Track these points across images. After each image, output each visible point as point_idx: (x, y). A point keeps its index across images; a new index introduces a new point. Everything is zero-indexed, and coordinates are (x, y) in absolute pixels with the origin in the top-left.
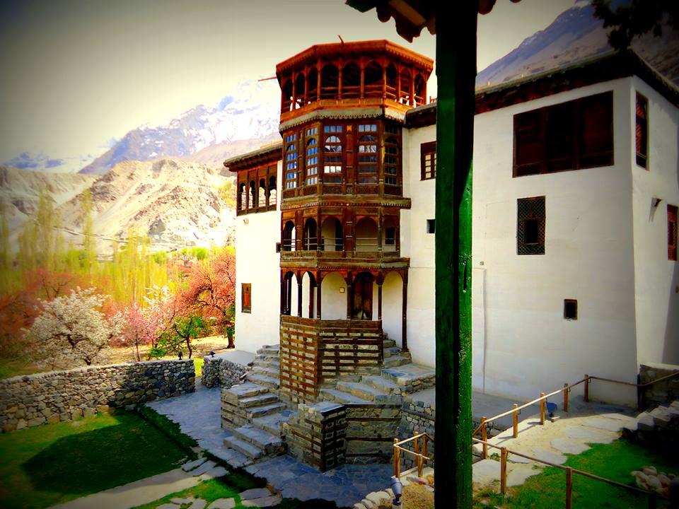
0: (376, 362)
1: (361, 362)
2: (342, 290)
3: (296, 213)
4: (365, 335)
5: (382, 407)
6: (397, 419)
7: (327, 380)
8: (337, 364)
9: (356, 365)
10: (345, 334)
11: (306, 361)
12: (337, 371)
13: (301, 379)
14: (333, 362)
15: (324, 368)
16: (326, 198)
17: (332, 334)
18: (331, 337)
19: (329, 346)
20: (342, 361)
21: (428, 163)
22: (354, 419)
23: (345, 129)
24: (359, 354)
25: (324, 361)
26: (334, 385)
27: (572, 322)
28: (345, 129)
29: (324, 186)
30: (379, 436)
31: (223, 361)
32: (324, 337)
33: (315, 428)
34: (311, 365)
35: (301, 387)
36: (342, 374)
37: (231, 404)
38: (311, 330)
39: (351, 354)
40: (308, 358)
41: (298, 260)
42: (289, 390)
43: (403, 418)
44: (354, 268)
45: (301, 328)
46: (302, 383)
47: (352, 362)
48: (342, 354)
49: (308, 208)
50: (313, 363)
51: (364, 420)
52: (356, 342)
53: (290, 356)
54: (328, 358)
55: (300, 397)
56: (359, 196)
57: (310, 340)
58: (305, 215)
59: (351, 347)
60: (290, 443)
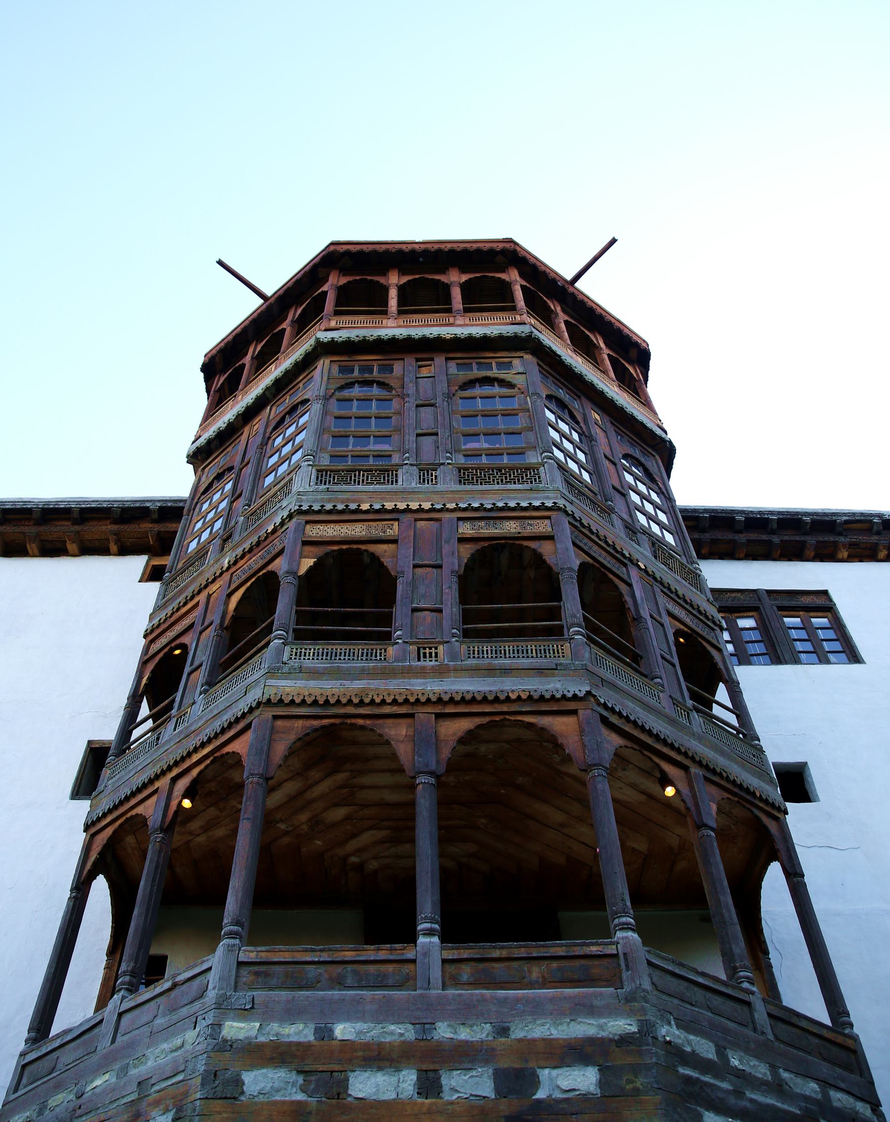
17: (706, 1049)
45: (466, 1013)
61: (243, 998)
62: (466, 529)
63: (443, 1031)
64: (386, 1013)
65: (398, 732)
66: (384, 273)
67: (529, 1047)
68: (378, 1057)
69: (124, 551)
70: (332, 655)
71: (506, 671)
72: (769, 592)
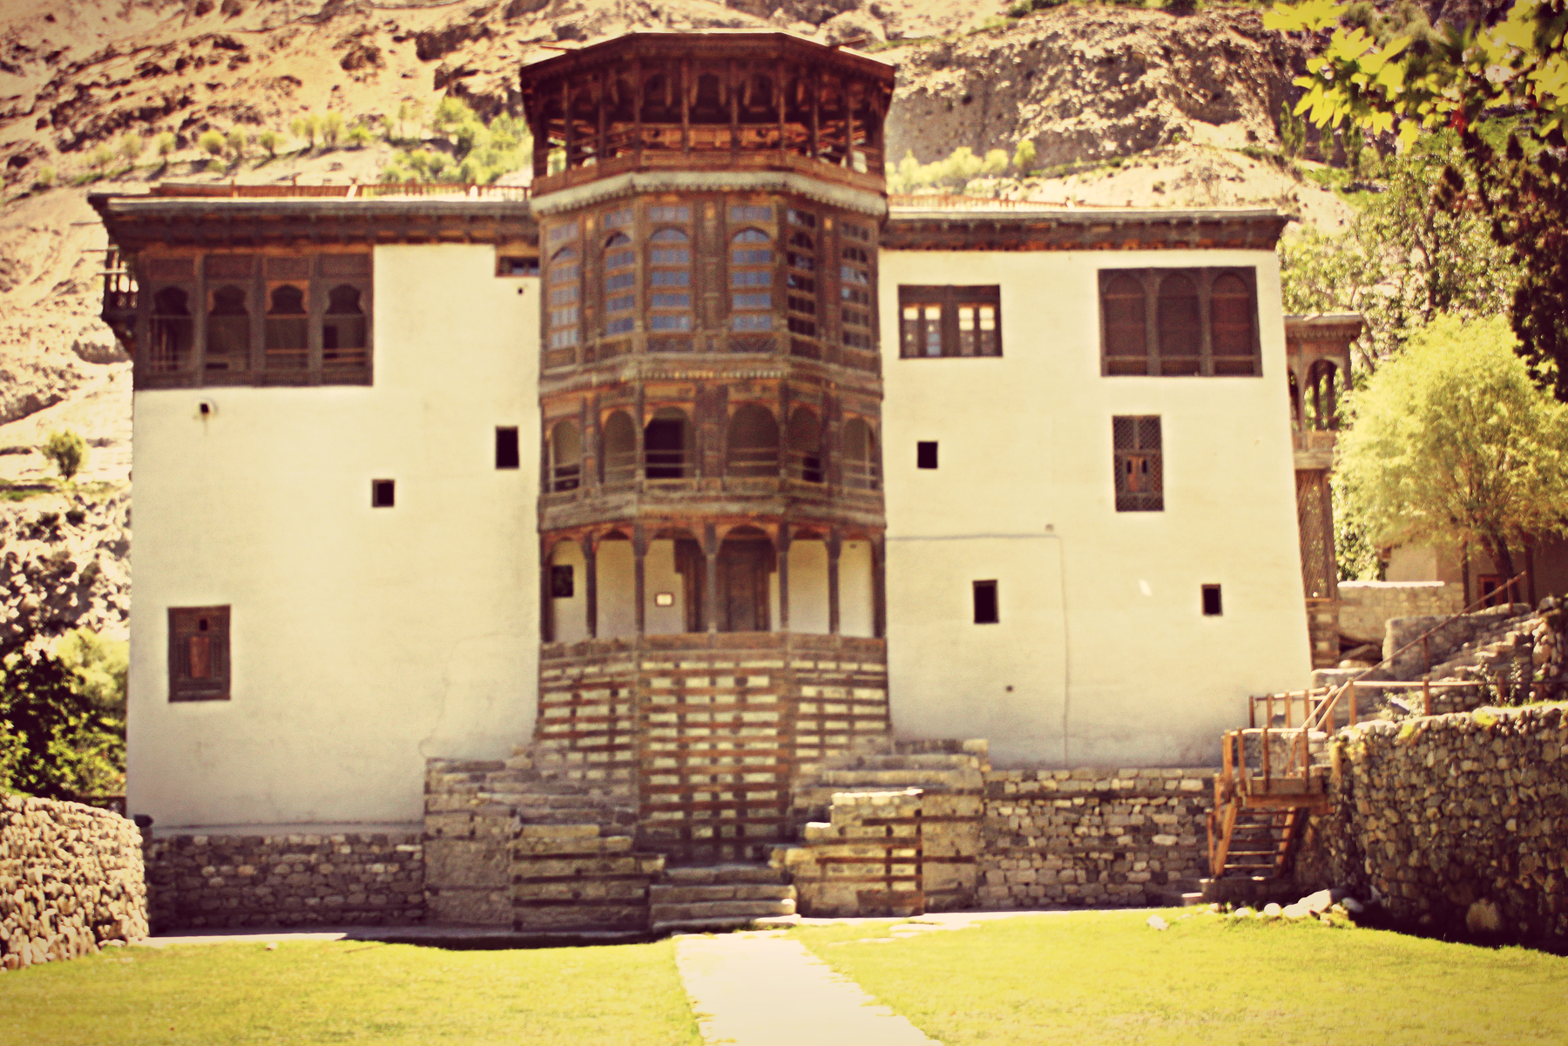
0: (880, 725)
1: (860, 725)
2: (664, 600)
3: (700, 390)
4: (867, 667)
5: (960, 792)
7: (807, 768)
8: (821, 732)
10: (832, 665)
11: (744, 732)
14: (812, 725)
15: (801, 740)
16: (800, 366)
17: (809, 665)
19: (809, 691)
20: (830, 725)
24: (857, 710)
25: (801, 725)
27: (1214, 619)
29: (794, 343)
30: (958, 852)
32: (799, 670)
34: (766, 739)
35: (727, 796)
38: (764, 657)
39: (842, 709)
40: (751, 725)
41: (717, 499)
42: (679, 815)
43: (992, 814)
45: (725, 658)
46: (728, 788)
47: (843, 725)
48: (830, 709)
50: (772, 732)
51: (935, 819)
52: (851, 682)
53: (680, 731)
54: (806, 717)
55: (727, 821)
57: (763, 681)
58: (734, 395)
59: (840, 693)
63: (719, 665)
64: (699, 659)
65: (699, 532)
68: (695, 673)
69: (474, 241)
70: (667, 488)
71: (748, 499)
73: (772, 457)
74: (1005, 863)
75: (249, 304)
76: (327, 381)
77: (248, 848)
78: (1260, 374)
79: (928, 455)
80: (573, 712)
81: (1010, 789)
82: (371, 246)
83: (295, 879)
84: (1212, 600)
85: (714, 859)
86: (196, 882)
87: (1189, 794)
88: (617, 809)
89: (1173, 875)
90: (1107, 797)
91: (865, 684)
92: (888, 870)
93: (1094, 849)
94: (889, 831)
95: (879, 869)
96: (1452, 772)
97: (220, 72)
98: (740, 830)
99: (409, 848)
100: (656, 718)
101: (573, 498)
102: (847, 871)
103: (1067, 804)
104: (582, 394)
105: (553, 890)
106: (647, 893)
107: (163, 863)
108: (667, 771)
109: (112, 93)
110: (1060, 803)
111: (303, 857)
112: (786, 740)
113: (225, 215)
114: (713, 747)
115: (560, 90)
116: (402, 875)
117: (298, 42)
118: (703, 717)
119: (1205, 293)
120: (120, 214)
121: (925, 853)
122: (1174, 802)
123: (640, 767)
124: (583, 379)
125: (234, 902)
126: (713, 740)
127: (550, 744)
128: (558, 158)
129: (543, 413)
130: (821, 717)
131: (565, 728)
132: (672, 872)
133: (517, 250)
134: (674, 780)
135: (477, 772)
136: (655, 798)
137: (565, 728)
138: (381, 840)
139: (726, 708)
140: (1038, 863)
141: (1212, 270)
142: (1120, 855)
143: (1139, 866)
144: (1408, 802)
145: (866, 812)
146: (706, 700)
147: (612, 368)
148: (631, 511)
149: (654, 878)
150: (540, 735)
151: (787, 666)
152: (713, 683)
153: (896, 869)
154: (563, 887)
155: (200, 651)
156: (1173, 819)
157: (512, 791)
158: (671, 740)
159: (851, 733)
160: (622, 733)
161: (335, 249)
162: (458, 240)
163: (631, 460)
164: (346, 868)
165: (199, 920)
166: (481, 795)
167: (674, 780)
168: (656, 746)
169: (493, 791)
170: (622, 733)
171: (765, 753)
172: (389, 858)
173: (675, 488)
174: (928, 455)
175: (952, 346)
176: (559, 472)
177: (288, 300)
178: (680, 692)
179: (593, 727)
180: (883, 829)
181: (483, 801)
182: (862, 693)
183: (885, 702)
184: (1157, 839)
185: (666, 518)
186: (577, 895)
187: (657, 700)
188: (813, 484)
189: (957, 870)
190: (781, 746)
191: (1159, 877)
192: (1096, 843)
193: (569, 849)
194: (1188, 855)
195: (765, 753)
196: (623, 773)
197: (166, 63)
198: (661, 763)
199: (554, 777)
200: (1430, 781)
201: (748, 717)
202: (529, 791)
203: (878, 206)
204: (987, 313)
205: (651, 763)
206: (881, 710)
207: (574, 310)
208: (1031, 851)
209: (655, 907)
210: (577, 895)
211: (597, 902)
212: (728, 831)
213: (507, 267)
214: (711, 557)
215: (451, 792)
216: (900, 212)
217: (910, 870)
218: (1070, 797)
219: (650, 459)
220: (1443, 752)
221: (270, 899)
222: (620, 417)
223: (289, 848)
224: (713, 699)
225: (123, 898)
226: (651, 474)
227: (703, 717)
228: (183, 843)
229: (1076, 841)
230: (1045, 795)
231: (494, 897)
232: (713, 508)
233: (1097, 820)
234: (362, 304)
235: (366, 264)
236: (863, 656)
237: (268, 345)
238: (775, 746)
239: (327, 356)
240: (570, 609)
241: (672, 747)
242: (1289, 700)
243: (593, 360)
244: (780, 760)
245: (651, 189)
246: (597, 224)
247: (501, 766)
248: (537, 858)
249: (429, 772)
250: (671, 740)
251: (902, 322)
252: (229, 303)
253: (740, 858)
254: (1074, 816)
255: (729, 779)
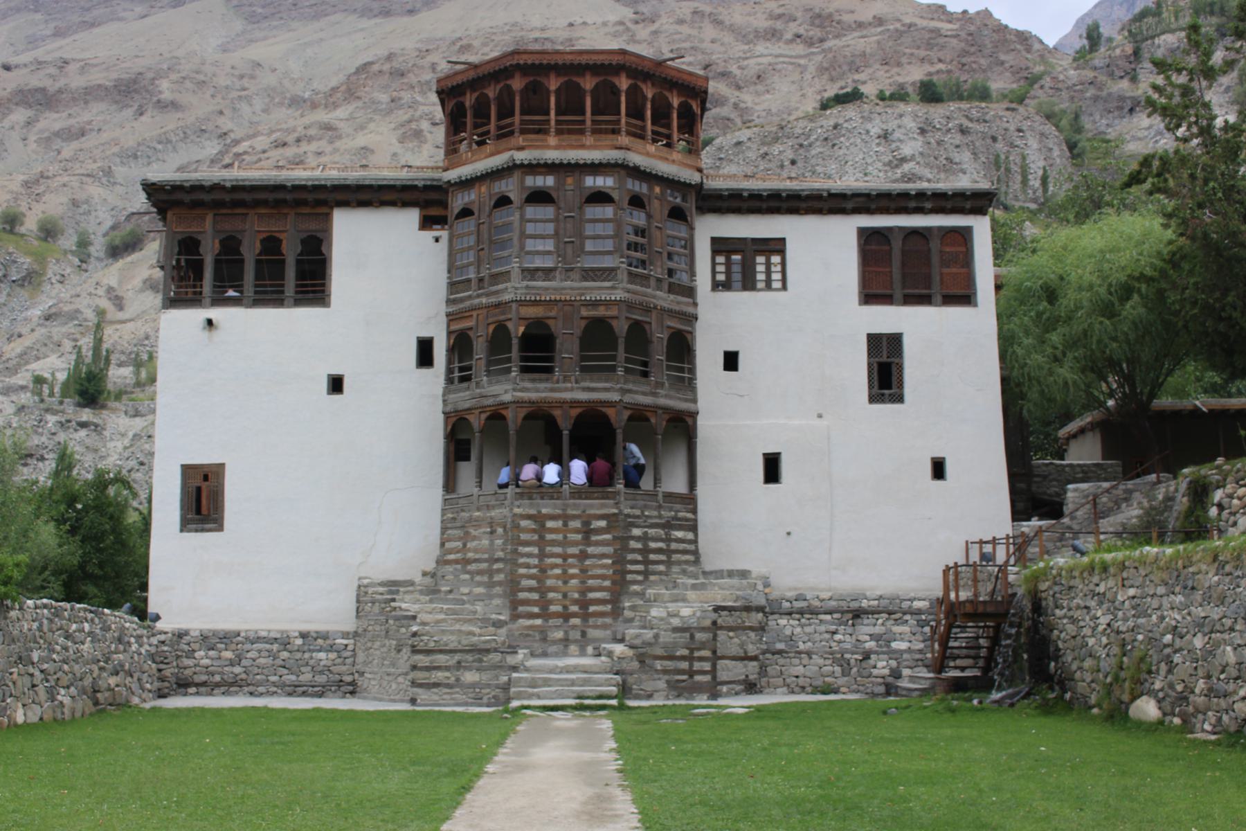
0: (690, 558)
1: (675, 557)
4: (681, 514)
5: (747, 609)
6: (761, 629)
7: (636, 588)
8: (646, 562)
9: (669, 563)
10: (655, 513)
11: (587, 562)
12: (646, 574)
13: (576, 596)
14: (640, 558)
15: (630, 567)
16: (634, 293)
17: (638, 512)
18: (638, 517)
19: (636, 532)
20: (652, 557)
21: (721, 268)
22: (721, 628)
23: (651, 189)
24: (674, 546)
25: (630, 557)
26: (641, 595)
28: (651, 189)
30: (746, 652)
31: (192, 634)
32: (628, 516)
33: (700, 636)
34: (604, 566)
35: (574, 608)
36: (652, 578)
37: (451, 651)
38: (603, 506)
40: (594, 556)
41: (572, 389)
42: (539, 622)
44: (666, 409)
45: (576, 506)
46: (575, 602)
47: (663, 557)
48: (653, 545)
49: (595, 304)
50: (610, 561)
51: (730, 629)
52: (668, 526)
53: (541, 560)
54: (634, 551)
55: (574, 627)
56: (672, 297)
57: (603, 523)
59: (661, 532)
60: (630, 680)
61: (517, 503)
62: (584, 312)
63: (570, 512)
64: (555, 507)
65: (557, 413)
66: (547, 76)
67: (590, 516)
68: (553, 517)
69: (405, 204)
70: (533, 381)
72: (753, 239)
73: (613, 358)
74: (781, 661)
75: (244, 250)
76: (298, 303)
77: (227, 638)
78: (976, 305)
79: (731, 362)
80: (465, 545)
81: (786, 605)
82: (332, 208)
83: (262, 661)
84: (939, 470)
85: (565, 654)
86: (190, 662)
87: (919, 612)
88: (494, 616)
89: (906, 672)
90: (858, 614)
91: (680, 528)
92: (691, 666)
93: (847, 651)
94: (692, 637)
95: (684, 665)
96: (1120, 598)
97: (323, 145)
98: (584, 634)
99: (345, 642)
100: (521, 549)
101: (468, 388)
102: (658, 665)
103: (828, 617)
104: (475, 313)
105: (439, 676)
106: (510, 679)
107: (166, 648)
108: (531, 590)
109: (255, 158)
110: (822, 617)
111: (268, 646)
112: (618, 567)
113: (228, 185)
114: (565, 572)
115: (465, 94)
116: (339, 661)
117: (372, 126)
118: (558, 550)
119: (935, 245)
120: (154, 184)
121: (719, 654)
122: (908, 617)
123: (513, 585)
124: (476, 301)
125: (217, 678)
126: (565, 568)
127: (449, 568)
128: (463, 147)
129: (448, 326)
130: (645, 551)
131: (459, 556)
132: (528, 664)
133: (434, 212)
134: (535, 596)
135: (393, 586)
136: (521, 609)
137: (459, 556)
138: (325, 636)
139: (575, 544)
140: (805, 660)
141: (940, 228)
142: (867, 656)
143: (880, 664)
144: (1083, 620)
145: (676, 622)
146: (560, 537)
147: (497, 292)
148: (507, 398)
149: (515, 668)
150: (441, 562)
151: (621, 513)
152: (565, 525)
153: (697, 666)
154: (447, 674)
155: (203, 499)
156: (906, 629)
157: (417, 601)
158: (535, 567)
159: (669, 563)
160: (497, 560)
161: (306, 210)
162: (392, 204)
163: (509, 360)
164: (299, 655)
165: (192, 690)
166: (393, 604)
167: (535, 596)
168: (522, 571)
169: (402, 600)
170: (497, 560)
171: (603, 577)
172: (331, 648)
173: (541, 381)
174: (731, 362)
175: (749, 284)
176: (461, 369)
177: (271, 245)
178: (541, 530)
179: (477, 556)
180: (688, 635)
181: (395, 608)
182: (679, 534)
183: (695, 542)
184: (894, 645)
185: (531, 402)
186: (458, 680)
187: (523, 536)
188: (643, 380)
189: (746, 666)
190: (614, 573)
191: (896, 674)
192: (848, 646)
193: (451, 646)
194: (918, 656)
195: (603, 577)
196: (498, 590)
197: (290, 139)
198: (526, 583)
199: (451, 591)
200: (1100, 603)
201: (590, 550)
202: (431, 601)
203: (695, 178)
204: (776, 259)
205: (519, 583)
206: (692, 547)
207: (472, 253)
208: (800, 653)
209: (513, 690)
210: (458, 680)
211: (473, 686)
212: (575, 635)
213: (427, 223)
214: (566, 432)
215: (373, 603)
216: (715, 184)
217: (707, 666)
218: (830, 613)
219: (523, 359)
220: (1111, 583)
221: (244, 676)
222: (501, 332)
223: (259, 639)
224: (565, 537)
225: (122, 673)
226: (524, 370)
227: (558, 550)
228: (181, 635)
229: (834, 644)
230: (814, 612)
231: (400, 679)
232: (568, 396)
233: (850, 630)
234: (324, 249)
235: (328, 218)
236: (678, 506)
237: (257, 277)
238: (611, 571)
239: (297, 286)
240: (466, 470)
241: (534, 571)
242: (994, 541)
243: (483, 288)
244: (614, 583)
245: (526, 162)
246: (489, 188)
247: (412, 583)
248: (429, 652)
249: (359, 586)
250: (535, 567)
251: (714, 264)
252: (230, 247)
253: (583, 653)
254: (833, 628)
255: (576, 596)
